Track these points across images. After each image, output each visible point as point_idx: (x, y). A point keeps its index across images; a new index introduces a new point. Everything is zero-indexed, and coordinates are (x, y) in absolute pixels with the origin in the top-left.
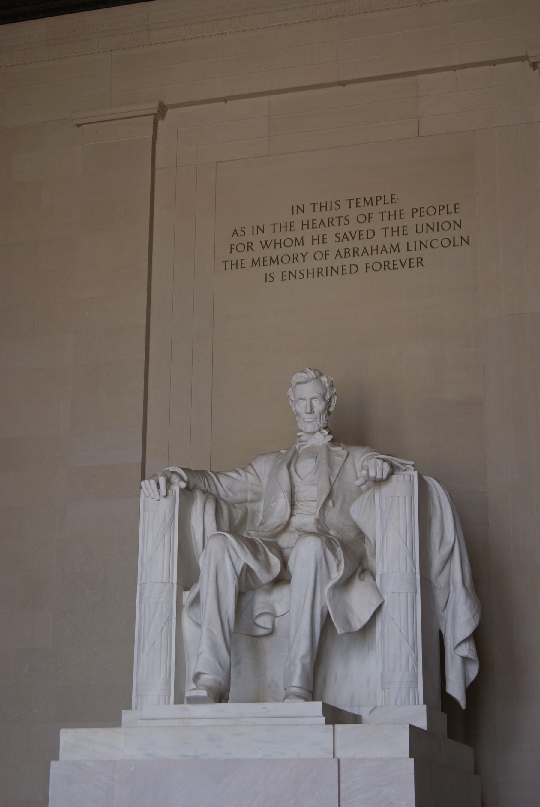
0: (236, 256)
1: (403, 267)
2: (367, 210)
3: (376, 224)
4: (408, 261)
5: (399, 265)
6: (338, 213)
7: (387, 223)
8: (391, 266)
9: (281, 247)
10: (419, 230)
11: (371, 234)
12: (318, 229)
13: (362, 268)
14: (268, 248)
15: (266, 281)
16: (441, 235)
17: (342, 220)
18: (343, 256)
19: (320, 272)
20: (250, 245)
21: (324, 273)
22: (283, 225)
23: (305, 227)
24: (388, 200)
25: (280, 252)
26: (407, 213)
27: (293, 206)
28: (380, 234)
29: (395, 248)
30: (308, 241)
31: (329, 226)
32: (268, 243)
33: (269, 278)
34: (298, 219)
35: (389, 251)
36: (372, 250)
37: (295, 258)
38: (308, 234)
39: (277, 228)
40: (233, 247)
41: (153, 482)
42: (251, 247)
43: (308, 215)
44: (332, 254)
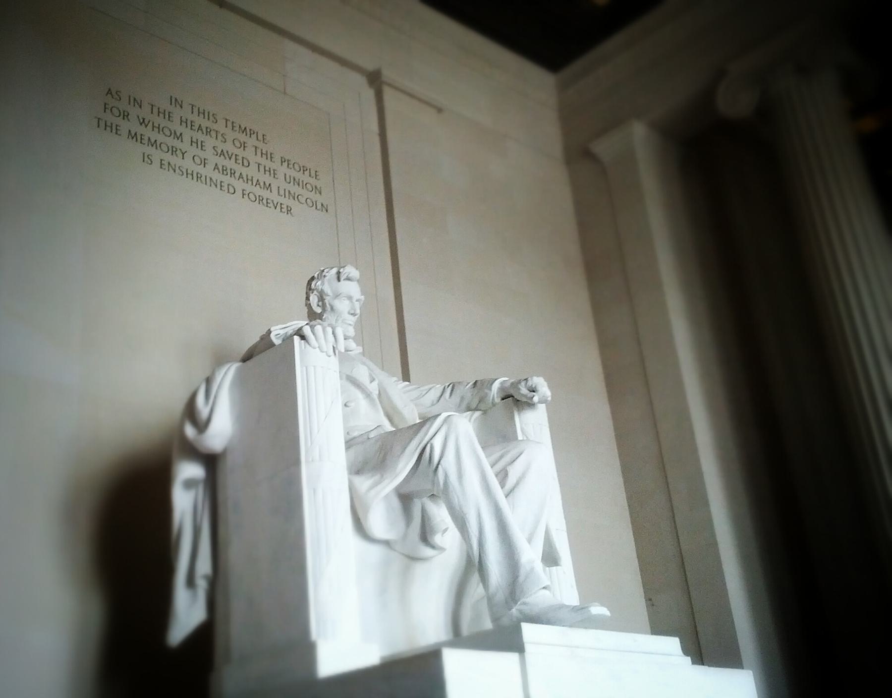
2: (243, 137)
3: (249, 154)
5: (271, 205)
6: (215, 127)
7: (259, 159)
8: (265, 201)
10: (288, 180)
13: (239, 193)
16: (306, 194)
19: (199, 177)
21: (203, 178)
23: (184, 124)
25: (160, 138)
26: (277, 159)
28: (253, 166)
30: (186, 138)
32: (146, 122)
33: (147, 159)
34: (177, 113)
37: (173, 151)
38: (187, 134)
39: (155, 110)
41: (329, 330)
43: (186, 113)
44: (210, 166)
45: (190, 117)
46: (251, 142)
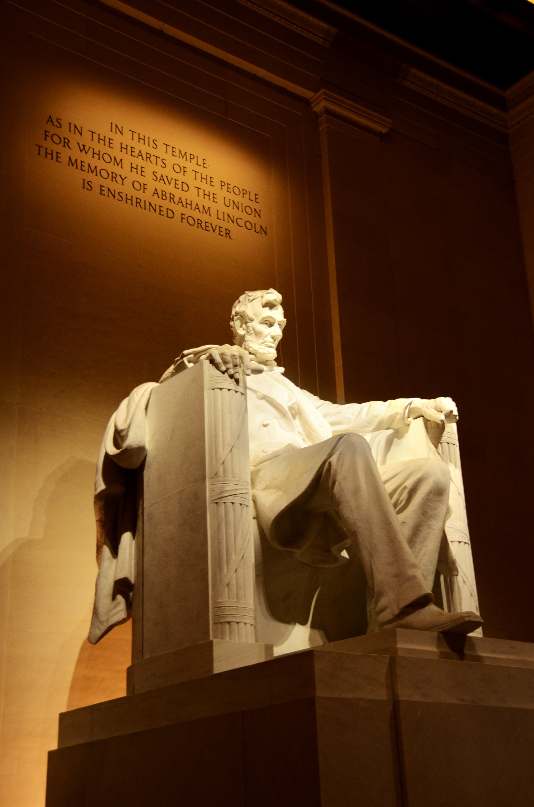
0: (49, 145)
1: (214, 231)
2: (182, 162)
4: (218, 228)
9: (99, 159)
10: (227, 204)
11: (185, 188)
12: (135, 158)
13: (178, 216)
14: (86, 153)
15: (84, 188)
17: (159, 160)
18: (160, 196)
20: (66, 141)
21: (142, 204)
22: (102, 137)
24: (200, 162)
25: (101, 165)
27: (112, 123)
29: (207, 211)
30: (126, 165)
31: (147, 161)
32: (87, 148)
34: (117, 139)
35: (201, 211)
36: (187, 204)
37: (114, 176)
38: (127, 159)
40: (47, 134)
42: (67, 143)
43: (126, 139)
44: (150, 190)
45: (131, 143)
46: (191, 166)
